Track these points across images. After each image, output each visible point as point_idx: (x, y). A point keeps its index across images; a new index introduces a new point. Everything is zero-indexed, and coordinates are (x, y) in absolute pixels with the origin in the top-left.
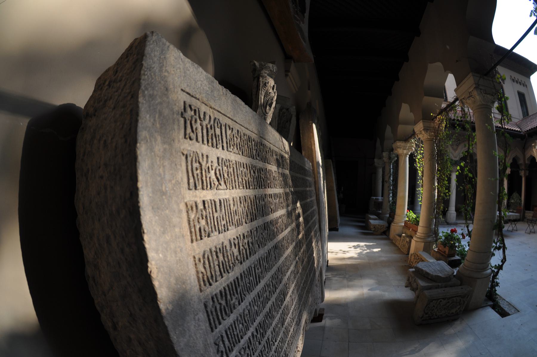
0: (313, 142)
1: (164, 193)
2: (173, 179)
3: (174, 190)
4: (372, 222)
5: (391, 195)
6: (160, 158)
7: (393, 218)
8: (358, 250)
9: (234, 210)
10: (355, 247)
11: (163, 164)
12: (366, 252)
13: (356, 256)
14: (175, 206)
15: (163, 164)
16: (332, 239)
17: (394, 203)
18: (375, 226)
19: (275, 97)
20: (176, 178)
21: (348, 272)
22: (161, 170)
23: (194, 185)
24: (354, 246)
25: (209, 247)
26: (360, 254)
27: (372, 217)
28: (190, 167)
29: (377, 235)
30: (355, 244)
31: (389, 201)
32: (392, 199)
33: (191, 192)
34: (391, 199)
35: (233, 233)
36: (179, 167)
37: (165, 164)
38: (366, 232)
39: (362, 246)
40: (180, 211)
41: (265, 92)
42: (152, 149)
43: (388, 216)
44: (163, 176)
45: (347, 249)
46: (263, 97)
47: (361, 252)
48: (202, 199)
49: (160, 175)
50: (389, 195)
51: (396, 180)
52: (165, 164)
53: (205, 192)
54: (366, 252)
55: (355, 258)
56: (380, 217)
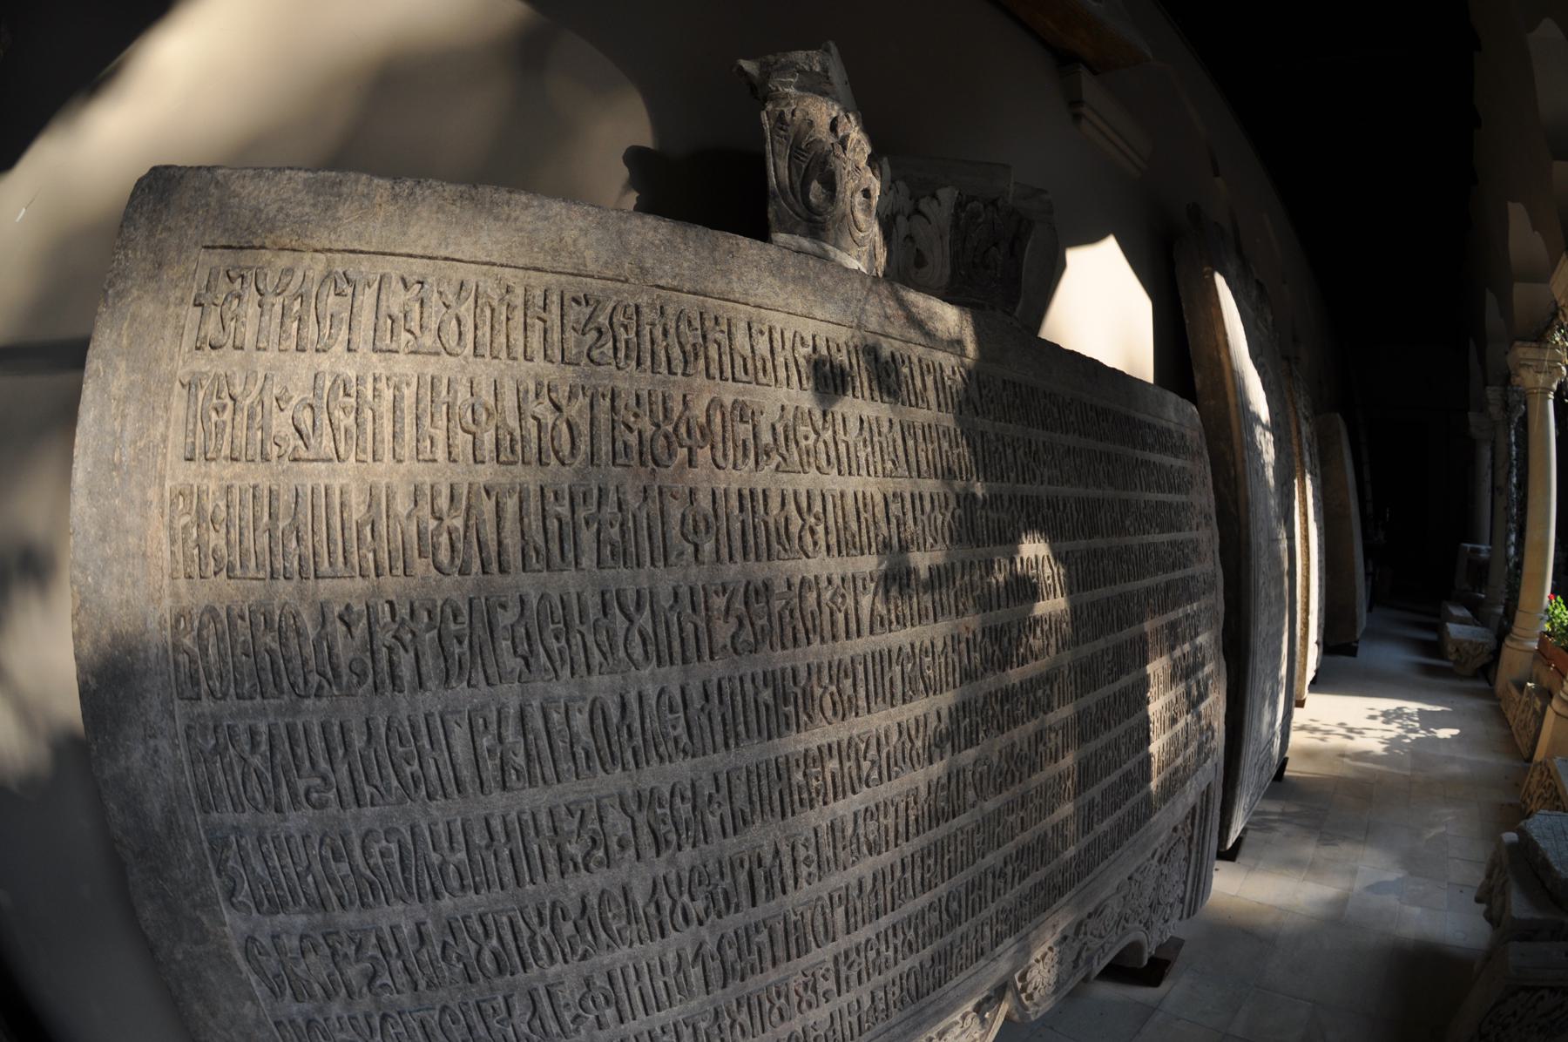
3: (140, 461)
8: (1394, 730)
12: (1413, 736)
13: (1378, 748)
14: (136, 492)
24: (1385, 714)
25: (227, 603)
26: (1394, 743)
33: (193, 465)
36: (159, 412)
39: (1409, 716)
40: (146, 504)
47: (1400, 737)
48: (224, 484)
54: (1413, 736)
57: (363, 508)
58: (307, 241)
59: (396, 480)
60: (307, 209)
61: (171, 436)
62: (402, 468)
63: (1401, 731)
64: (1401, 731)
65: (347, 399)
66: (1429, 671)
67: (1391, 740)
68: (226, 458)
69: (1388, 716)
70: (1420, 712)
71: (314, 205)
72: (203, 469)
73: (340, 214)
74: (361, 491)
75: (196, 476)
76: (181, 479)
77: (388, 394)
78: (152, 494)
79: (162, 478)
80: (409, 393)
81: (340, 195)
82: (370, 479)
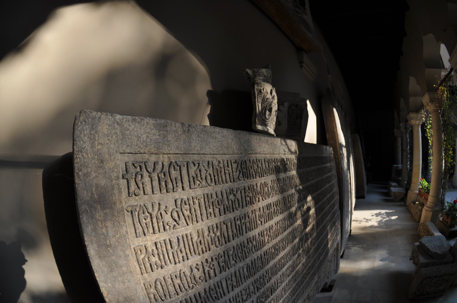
0: (334, 125)
1: (110, 246)
2: (117, 234)
3: (119, 242)
4: (393, 189)
5: (409, 163)
6: (102, 221)
7: (410, 186)
8: (379, 218)
9: (199, 240)
10: (377, 215)
11: (105, 225)
12: (385, 219)
13: (376, 224)
15: (105, 225)
16: (358, 207)
17: (411, 170)
18: (395, 194)
19: (276, 101)
20: (120, 233)
21: (367, 241)
22: (104, 230)
23: (143, 232)
26: (380, 222)
27: (393, 184)
28: (136, 220)
29: (396, 202)
30: (377, 211)
31: (407, 169)
32: (410, 167)
34: (409, 166)
35: (195, 260)
37: (107, 225)
38: (388, 200)
39: (383, 214)
41: (261, 99)
42: (93, 217)
43: (406, 182)
44: (106, 234)
45: (369, 217)
46: (260, 105)
47: (381, 220)
48: (154, 242)
49: (104, 234)
50: (407, 163)
51: (412, 149)
52: (107, 225)
53: (157, 235)
54: (385, 219)
55: (376, 227)
56: (400, 184)
57: (197, 237)
58: (161, 151)
59: (203, 227)
60: (157, 137)
61: (128, 230)
62: (204, 223)
63: (381, 219)
64: (381, 219)
65: (186, 206)
66: (387, 201)
67: (379, 221)
68: (152, 234)
69: (377, 215)
70: (386, 213)
71: (159, 135)
72: (144, 239)
73: (169, 139)
74: (195, 233)
75: (142, 242)
76: (137, 244)
77: (197, 202)
78: (128, 252)
79: (130, 246)
80: (202, 200)
81: (167, 131)
82: (197, 228)
